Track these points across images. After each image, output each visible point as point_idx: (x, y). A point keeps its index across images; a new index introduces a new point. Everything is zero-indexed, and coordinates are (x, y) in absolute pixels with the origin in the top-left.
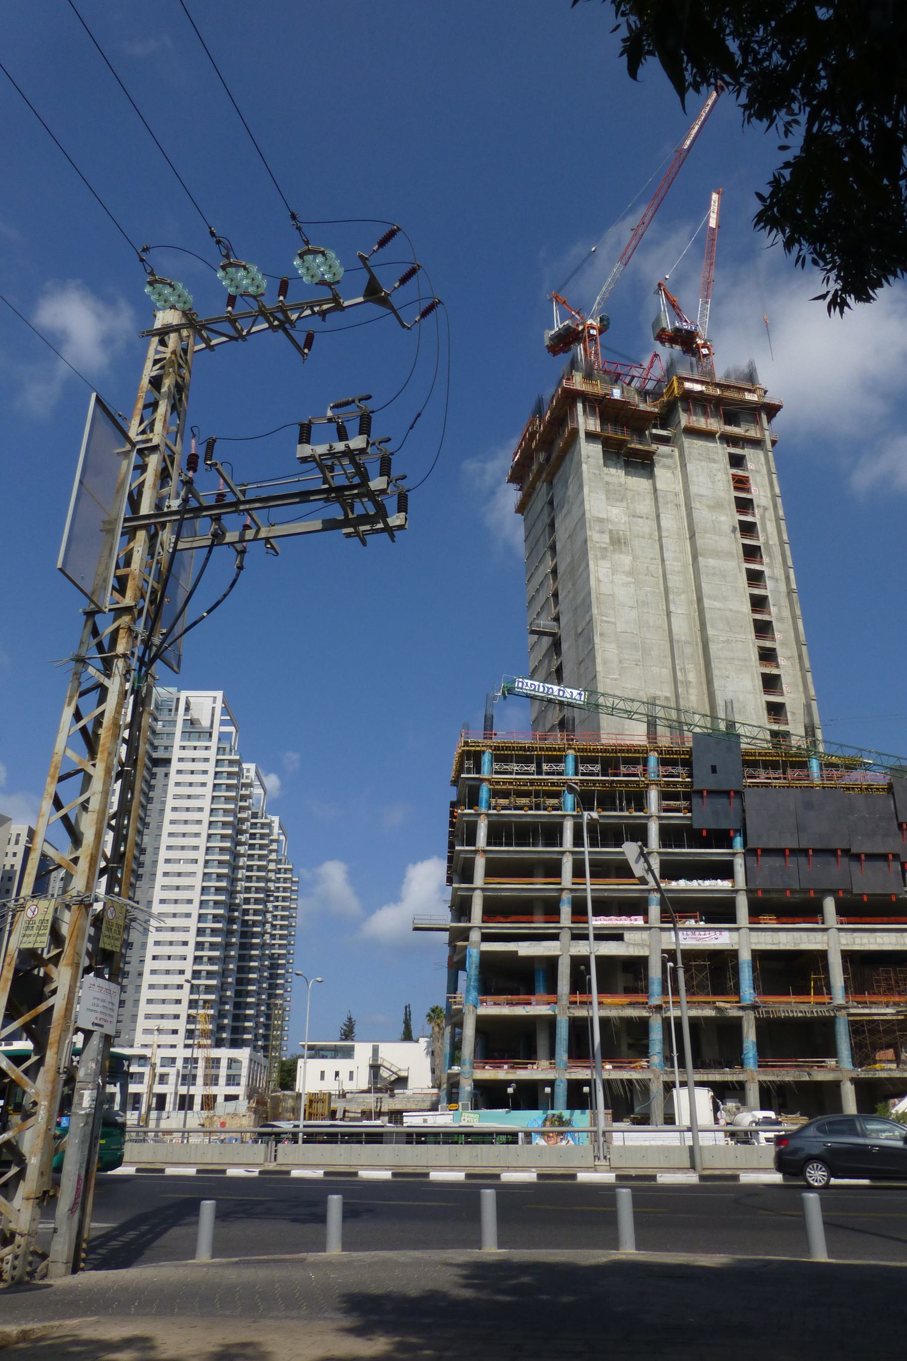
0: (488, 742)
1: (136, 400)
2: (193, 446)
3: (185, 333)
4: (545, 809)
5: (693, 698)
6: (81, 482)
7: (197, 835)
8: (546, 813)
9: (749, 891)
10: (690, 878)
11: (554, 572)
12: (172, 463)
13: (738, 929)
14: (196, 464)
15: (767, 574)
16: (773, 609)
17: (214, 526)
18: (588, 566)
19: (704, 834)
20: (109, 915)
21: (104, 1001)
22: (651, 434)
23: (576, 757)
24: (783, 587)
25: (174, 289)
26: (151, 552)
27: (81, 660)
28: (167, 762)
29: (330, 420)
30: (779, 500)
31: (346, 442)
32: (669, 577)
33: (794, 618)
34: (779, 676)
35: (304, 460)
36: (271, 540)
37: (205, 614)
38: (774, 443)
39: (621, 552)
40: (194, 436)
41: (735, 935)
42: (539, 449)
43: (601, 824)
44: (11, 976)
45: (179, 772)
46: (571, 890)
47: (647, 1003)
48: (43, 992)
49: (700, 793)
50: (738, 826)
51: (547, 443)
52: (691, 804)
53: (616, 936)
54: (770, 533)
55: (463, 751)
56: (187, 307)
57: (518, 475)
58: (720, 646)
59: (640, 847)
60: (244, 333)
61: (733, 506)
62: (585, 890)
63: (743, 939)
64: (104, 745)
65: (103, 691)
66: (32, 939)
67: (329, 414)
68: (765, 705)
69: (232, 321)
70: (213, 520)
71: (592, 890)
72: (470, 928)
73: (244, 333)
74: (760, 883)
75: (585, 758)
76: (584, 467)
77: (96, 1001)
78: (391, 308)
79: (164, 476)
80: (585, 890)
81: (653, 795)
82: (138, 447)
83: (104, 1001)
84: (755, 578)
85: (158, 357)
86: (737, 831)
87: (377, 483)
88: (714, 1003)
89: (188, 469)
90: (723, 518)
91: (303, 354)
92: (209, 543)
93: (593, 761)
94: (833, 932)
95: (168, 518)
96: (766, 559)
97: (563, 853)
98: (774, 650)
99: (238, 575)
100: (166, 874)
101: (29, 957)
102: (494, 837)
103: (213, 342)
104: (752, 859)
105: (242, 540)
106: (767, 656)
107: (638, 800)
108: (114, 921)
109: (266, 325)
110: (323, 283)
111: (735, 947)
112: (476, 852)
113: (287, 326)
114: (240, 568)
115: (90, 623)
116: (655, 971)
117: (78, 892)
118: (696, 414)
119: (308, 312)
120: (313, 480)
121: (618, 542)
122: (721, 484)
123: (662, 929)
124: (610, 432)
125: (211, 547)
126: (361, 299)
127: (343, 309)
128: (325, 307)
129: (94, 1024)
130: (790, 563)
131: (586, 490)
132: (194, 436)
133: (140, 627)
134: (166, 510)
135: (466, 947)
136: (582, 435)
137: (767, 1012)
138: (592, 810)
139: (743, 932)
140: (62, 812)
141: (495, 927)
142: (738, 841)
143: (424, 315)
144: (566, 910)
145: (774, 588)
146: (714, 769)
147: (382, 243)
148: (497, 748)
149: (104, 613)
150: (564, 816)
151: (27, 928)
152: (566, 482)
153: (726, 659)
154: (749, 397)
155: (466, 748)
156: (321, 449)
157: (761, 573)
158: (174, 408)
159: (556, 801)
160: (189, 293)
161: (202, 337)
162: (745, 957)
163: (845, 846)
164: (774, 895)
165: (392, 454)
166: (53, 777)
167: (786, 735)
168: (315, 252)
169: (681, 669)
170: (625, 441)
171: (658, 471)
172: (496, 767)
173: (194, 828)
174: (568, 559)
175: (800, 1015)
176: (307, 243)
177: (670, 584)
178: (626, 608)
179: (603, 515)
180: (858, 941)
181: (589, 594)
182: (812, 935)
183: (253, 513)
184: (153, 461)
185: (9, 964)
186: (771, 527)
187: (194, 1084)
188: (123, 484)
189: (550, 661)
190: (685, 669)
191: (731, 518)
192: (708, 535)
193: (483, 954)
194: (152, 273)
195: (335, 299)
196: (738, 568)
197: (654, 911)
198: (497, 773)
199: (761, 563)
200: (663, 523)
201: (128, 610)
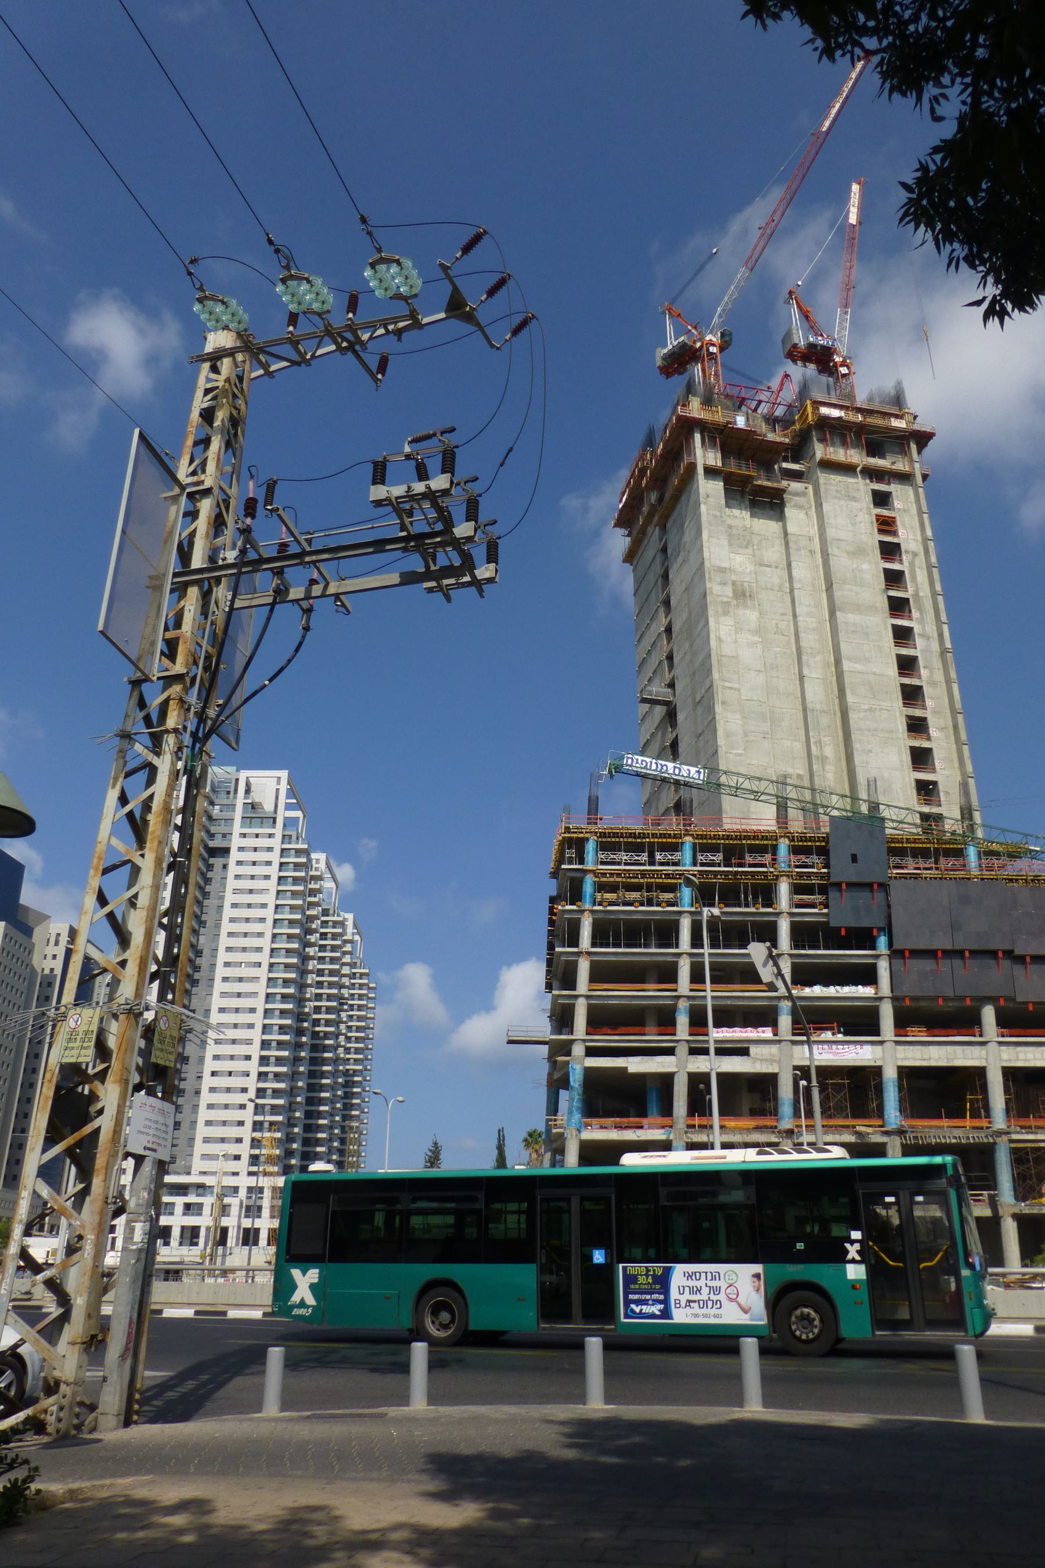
0: (593, 828)
1: (184, 436)
2: (252, 489)
3: (240, 357)
4: (659, 905)
5: (830, 776)
6: (123, 531)
7: (260, 935)
8: (659, 909)
9: (894, 999)
10: (826, 984)
11: (669, 630)
12: (227, 509)
13: (882, 1043)
14: (254, 509)
15: (916, 631)
16: (924, 672)
17: (276, 581)
18: (707, 623)
19: (843, 932)
20: (162, 1025)
21: (157, 1122)
22: (780, 468)
23: (694, 844)
24: (935, 646)
25: (227, 307)
26: (205, 612)
27: (126, 736)
28: (225, 851)
29: (408, 457)
30: (931, 545)
31: (427, 482)
32: (802, 635)
33: (948, 681)
34: (930, 750)
35: (378, 503)
36: (342, 597)
37: (267, 682)
38: (925, 477)
39: (746, 607)
40: (252, 477)
41: (878, 1049)
42: (650, 487)
43: (723, 921)
44: (51, 1094)
45: (239, 863)
46: (689, 997)
47: (776, 1127)
48: (87, 1113)
49: (838, 885)
50: (882, 923)
51: (660, 481)
52: (827, 898)
53: (741, 1050)
54: (920, 584)
55: (564, 838)
56: (242, 327)
57: (625, 519)
58: (862, 715)
59: (769, 948)
60: (308, 357)
61: (877, 552)
62: (705, 997)
63: (888, 1054)
64: (153, 832)
65: (152, 771)
66: (75, 1052)
67: (407, 449)
68: (913, 784)
69: (294, 342)
70: (274, 574)
71: (713, 997)
72: (573, 1041)
73: (308, 357)
74: (907, 989)
75: (704, 846)
76: (703, 508)
77: (147, 1123)
78: (478, 325)
79: (218, 523)
80: (705, 997)
81: (784, 888)
82: (188, 490)
83: (157, 1122)
84: (902, 635)
85: (209, 386)
86: (881, 929)
87: (463, 529)
88: (854, 1127)
89: (246, 516)
90: (865, 566)
91: (376, 380)
92: (270, 600)
93: (713, 849)
94: (992, 1046)
95: (224, 573)
96: (915, 614)
97: (679, 955)
98: (924, 719)
99: (304, 637)
100: (225, 979)
101: (72, 1072)
102: (600, 937)
103: (273, 368)
104: (898, 963)
105: (308, 597)
106: (917, 726)
107: (766, 894)
108: (168, 1033)
109: (333, 347)
110: (398, 296)
111: (878, 1063)
112: (579, 954)
113: (357, 347)
114: (307, 629)
115: (136, 694)
116: (785, 1091)
117: (127, 999)
118: (833, 445)
119: (381, 331)
120: (389, 526)
121: (742, 595)
122: (862, 525)
123: (794, 1043)
124: (733, 467)
125: (272, 605)
126: (442, 315)
127: (421, 326)
128: (401, 325)
129: (145, 1148)
130: (944, 618)
131: (705, 535)
132: (252, 477)
133: (193, 698)
134: (220, 562)
135: (568, 1063)
136: (700, 470)
137: (916, 1138)
138: (712, 905)
139: (888, 1046)
140: (107, 909)
141: (602, 1040)
142: (882, 941)
143: (516, 332)
144: (683, 1021)
145: (925, 647)
146: (854, 858)
147: (467, 249)
148: (603, 835)
149: (152, 681)
150: (681, 913)
151: (70, 1040)
152: (682, 525)
153: (869, 730)
154: (895, 423)
155: (567, 835)
156: (398, 491)
157: (910, 630)
158: (228, 445)
159: (671, 895)
160: (245, 311)
161: (259, 362)
162: (890, 1074)
163: (1008, 947)
164: (923, 1004)
165: (480, 495)
166: (97, 869)
167: (939, 818)
168: (388, 261)
169: (816, 743)
170: (750, 478)
171: (789, 512)
172: (602, 856)
174: (685, 616)
175: (954, 1141)
176: (379, 250)
177: (803, 644)
178: (752, 672)
179: (727, 565)
180: (1021, 1056)
181: (709, 656)
182: (968, 1049)
183: (321, 565)
184: (206, 506)
185: (50, 1081)
186: (922, 576)
187: (259, 1217)
188: (171, 533)
189: (664, 734)
190: (820, 741)
191: (874, 567)
192: (847, 587)
193: (588, 1071)
194: (201, 289)
195: (413, 315)
196: (883, 624)
197: (785, 1021)
198: (603, 863)
199: (910, 618)
200: (794, 573)
201: (178, 678)
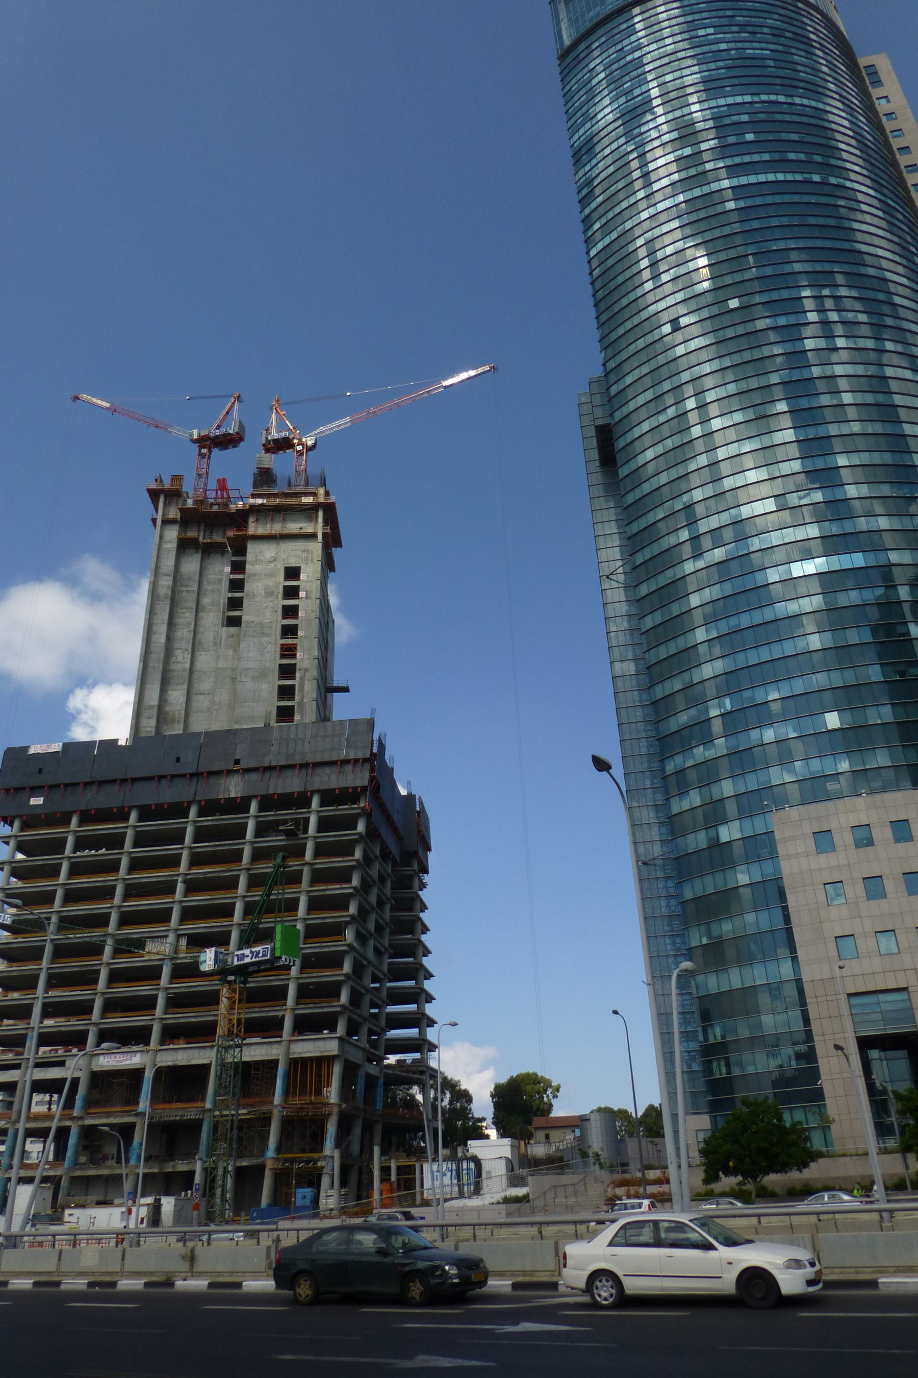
90: (264, 686)
122: (269, 655)
162: (149, 1075)
175: (178, 1118)
192: (246, 704)
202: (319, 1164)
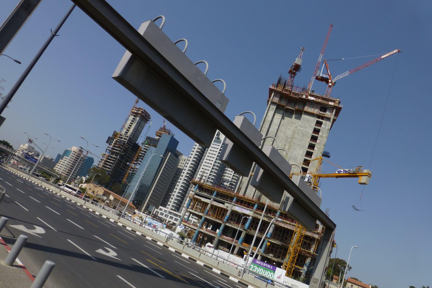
7: (210, 167)
45: (210, 150)
106: (312, 146)
116: (228, 214)
123: (234, 205)
162: (251, 218)
173: (209, 165)
202: (301, 271)
